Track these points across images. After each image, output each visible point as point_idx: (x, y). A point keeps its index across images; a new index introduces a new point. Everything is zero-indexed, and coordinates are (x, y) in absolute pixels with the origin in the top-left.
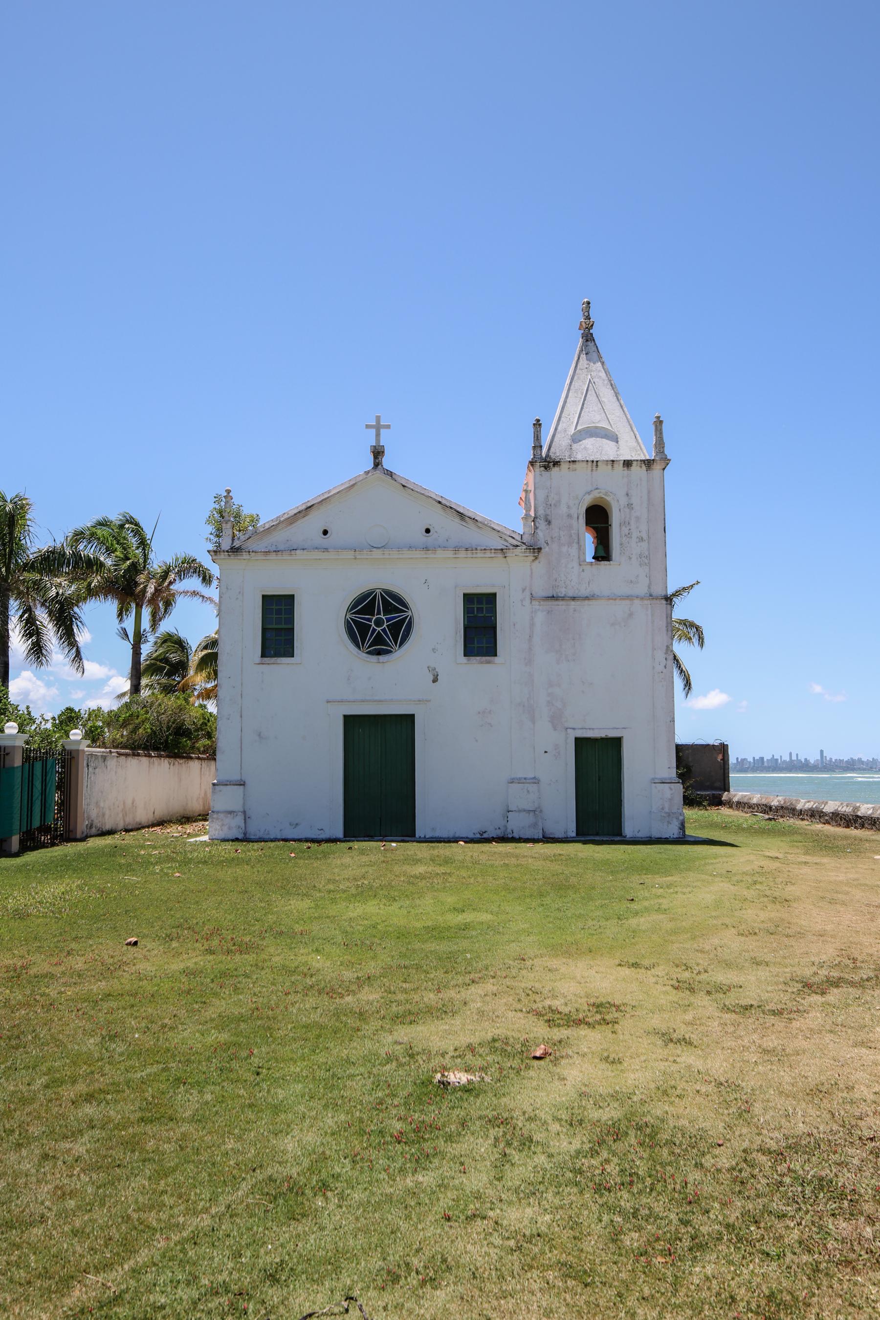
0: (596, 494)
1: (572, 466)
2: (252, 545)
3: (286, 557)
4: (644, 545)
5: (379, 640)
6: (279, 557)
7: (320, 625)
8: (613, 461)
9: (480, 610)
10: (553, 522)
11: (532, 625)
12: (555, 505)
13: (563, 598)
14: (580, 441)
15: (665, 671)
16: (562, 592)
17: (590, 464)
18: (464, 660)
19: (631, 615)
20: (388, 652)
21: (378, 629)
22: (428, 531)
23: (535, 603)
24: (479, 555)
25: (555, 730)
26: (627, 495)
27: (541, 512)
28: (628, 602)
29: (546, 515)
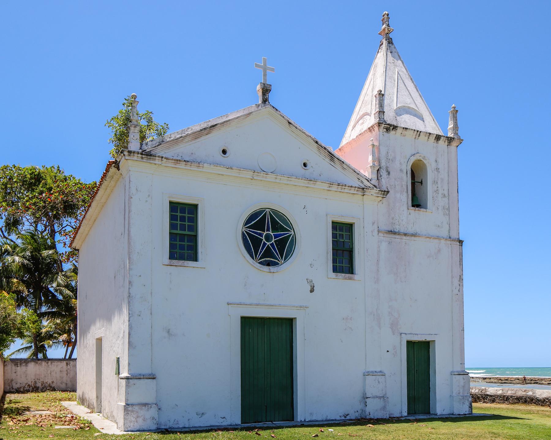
0: (417, 157)
1: (405, 132)
2: (159, 151)
3: (194, 168)
4: (446, 200)
5: (268, 253)
6: (188, 167)
7: (220, 233)
8: (430, 134)
9: (342, 236)
10: (391, 174)
11: (379, 251)
12: (392, 161)
13: (398, 233)
14: (401, 115)
15: (458, 293)
16: (397, 228)
17: (416, 132)
18: (333, 275)
19: (439, 251)
20: (275, 264)
21: (268, 243)
22: (305, 165)
23: (380, 234)
24: (346, 191)
25: (394, 334)
26: (436, 161)
27: (383, 164)
28: (437, 241)
29: (387, 167)
